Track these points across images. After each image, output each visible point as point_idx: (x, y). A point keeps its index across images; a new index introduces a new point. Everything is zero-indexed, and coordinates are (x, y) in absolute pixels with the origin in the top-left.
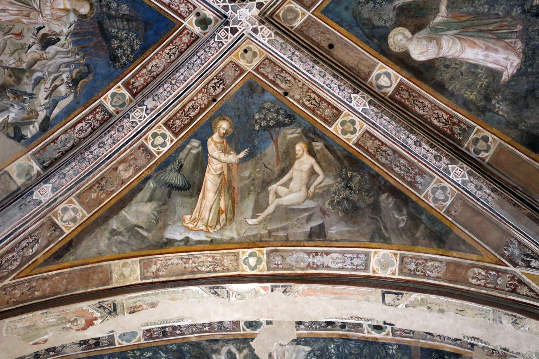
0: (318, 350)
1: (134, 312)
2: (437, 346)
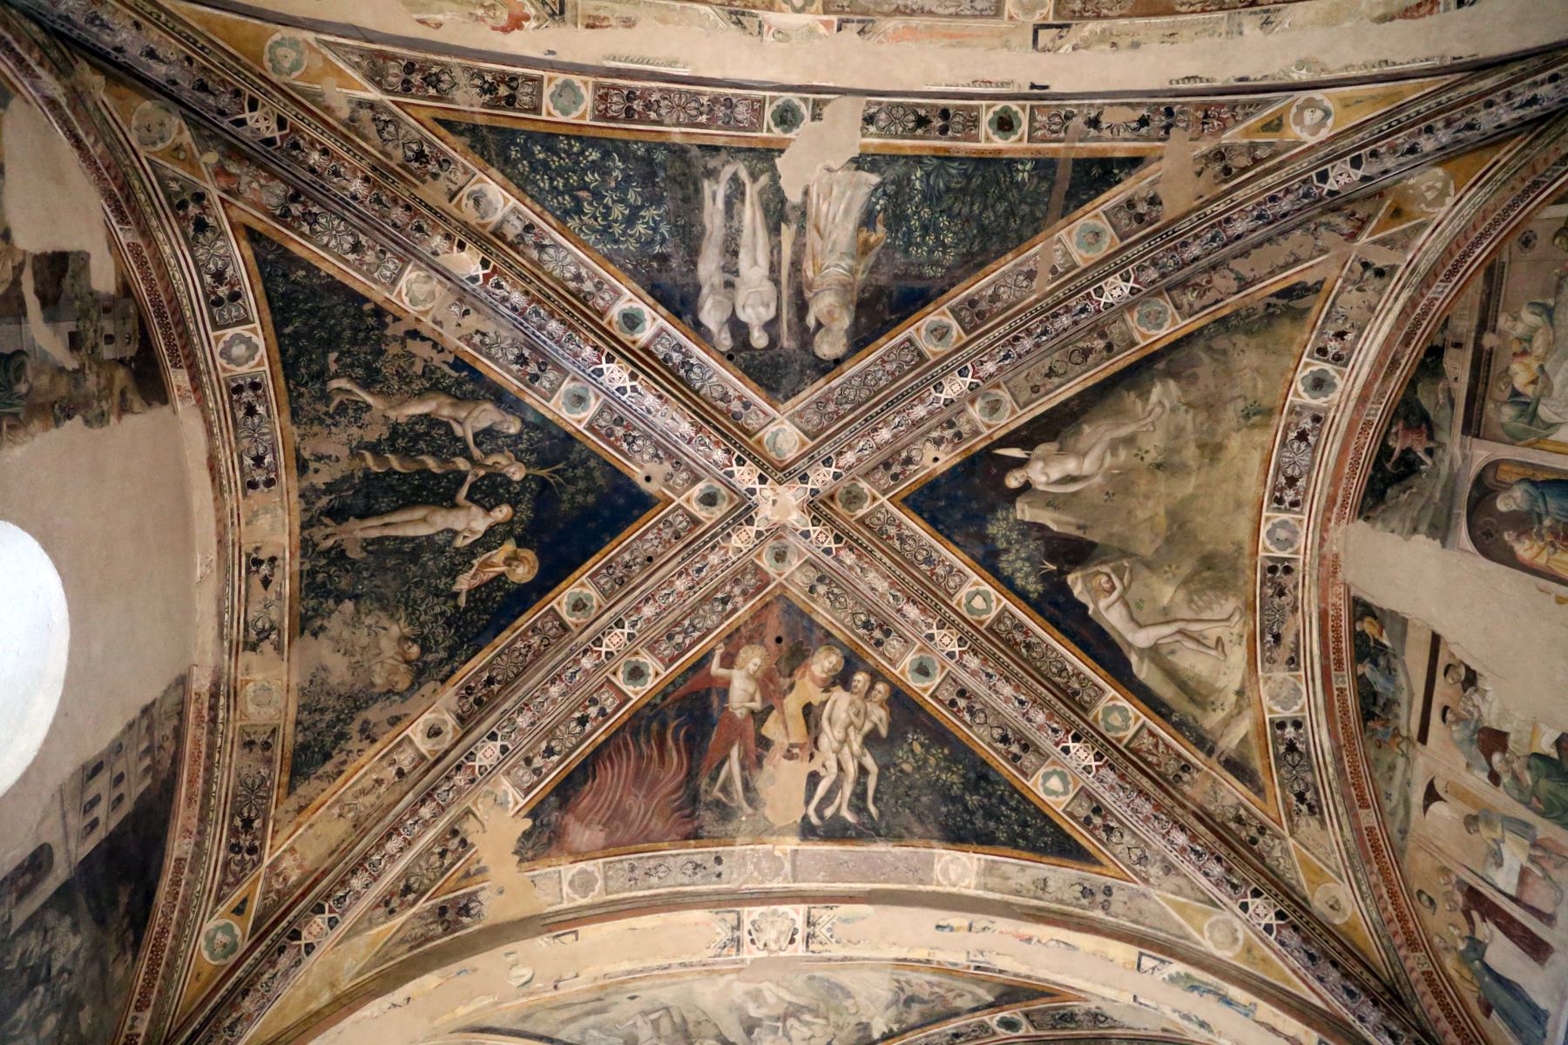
0: (893, 183)
1: (592, 27)
2: (1104, 149)
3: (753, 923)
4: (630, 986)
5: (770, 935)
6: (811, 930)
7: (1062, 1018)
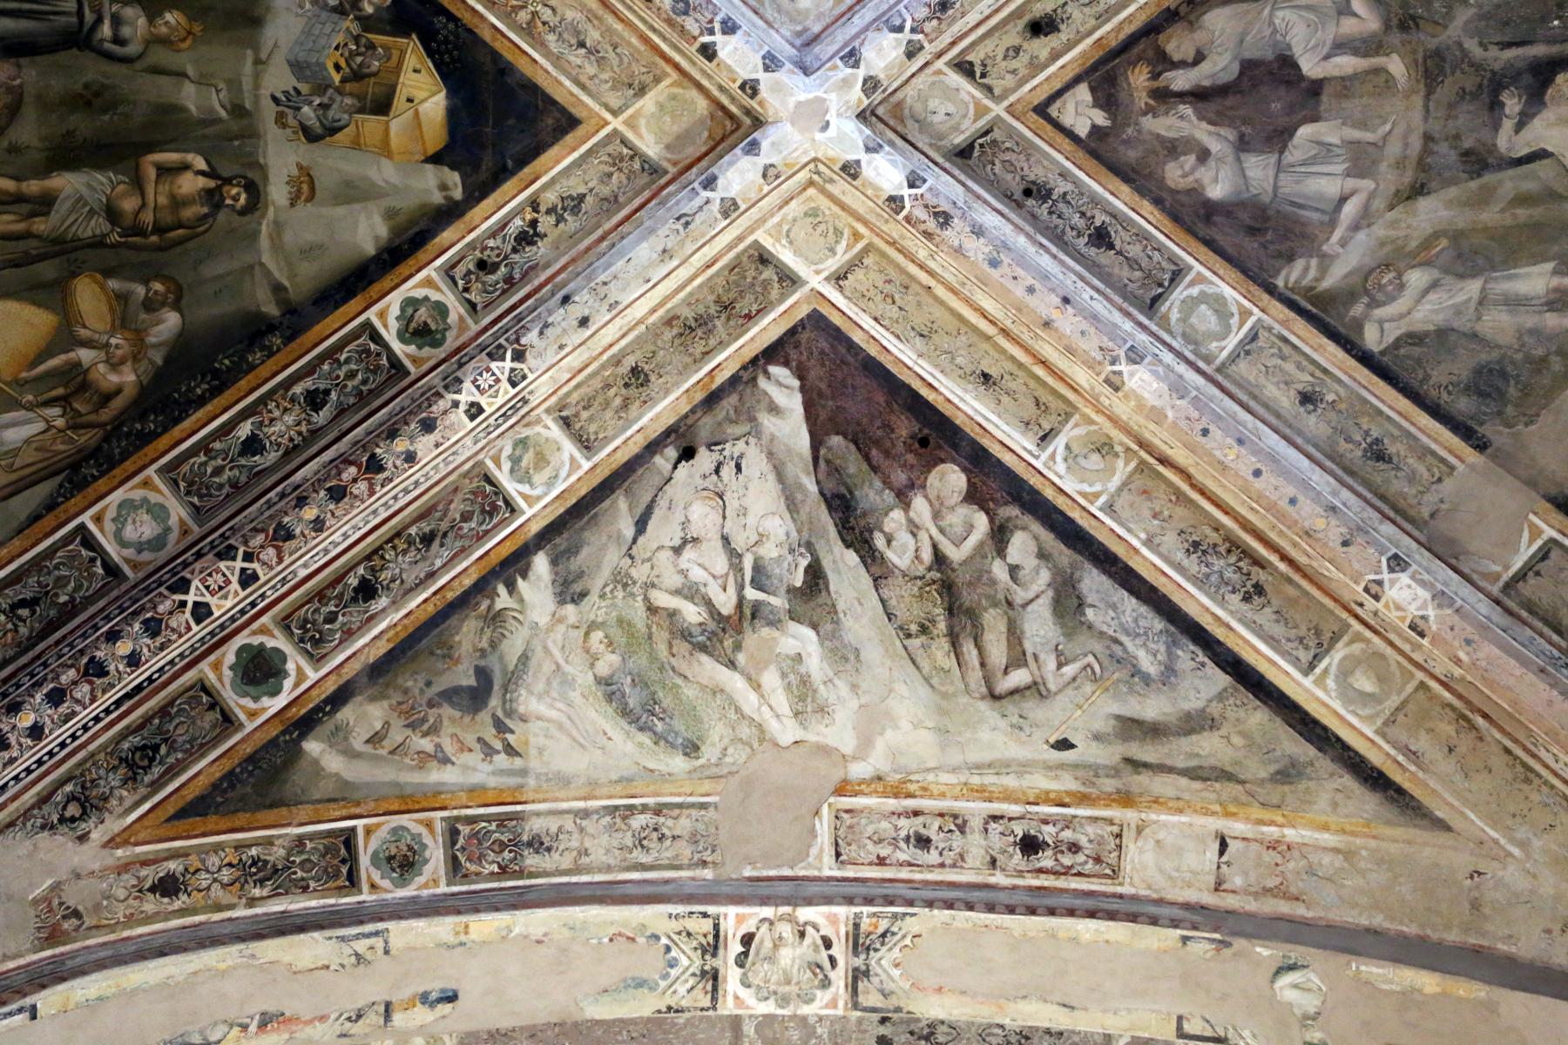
3: (826, 983)
4: (1067, 783)
5: (791, 956)
6: (711, 963)
7: (149, 752)
